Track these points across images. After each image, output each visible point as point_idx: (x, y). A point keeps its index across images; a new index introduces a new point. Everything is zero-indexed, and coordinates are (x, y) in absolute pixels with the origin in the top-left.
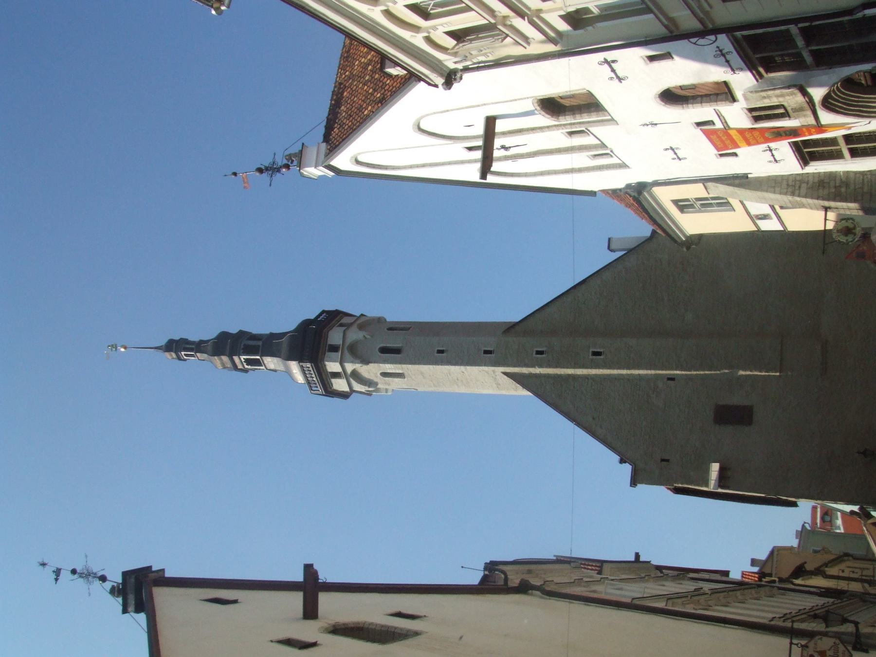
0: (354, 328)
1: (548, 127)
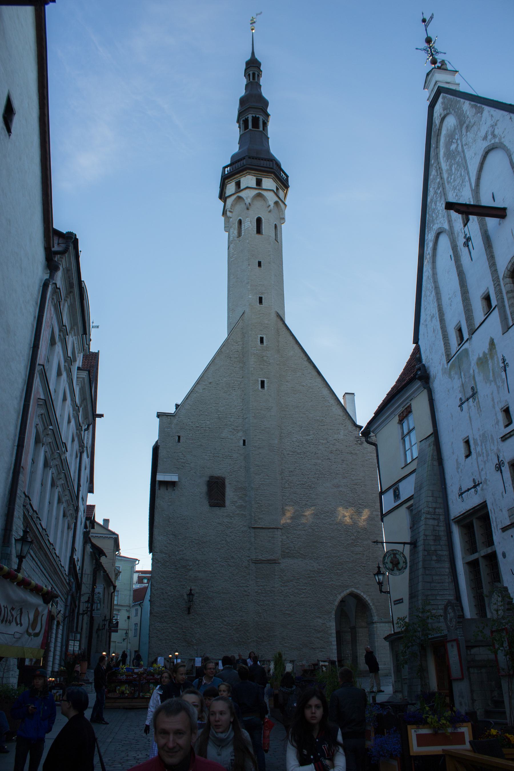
0: (276, 199)
1: (496, 271)
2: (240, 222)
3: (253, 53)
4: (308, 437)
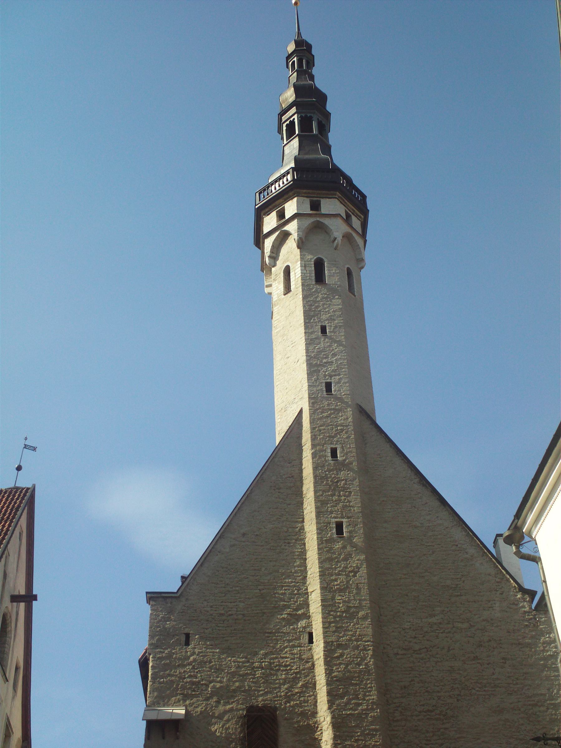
0: (345, 228)
3: (299, 34)
4: (434, 620)
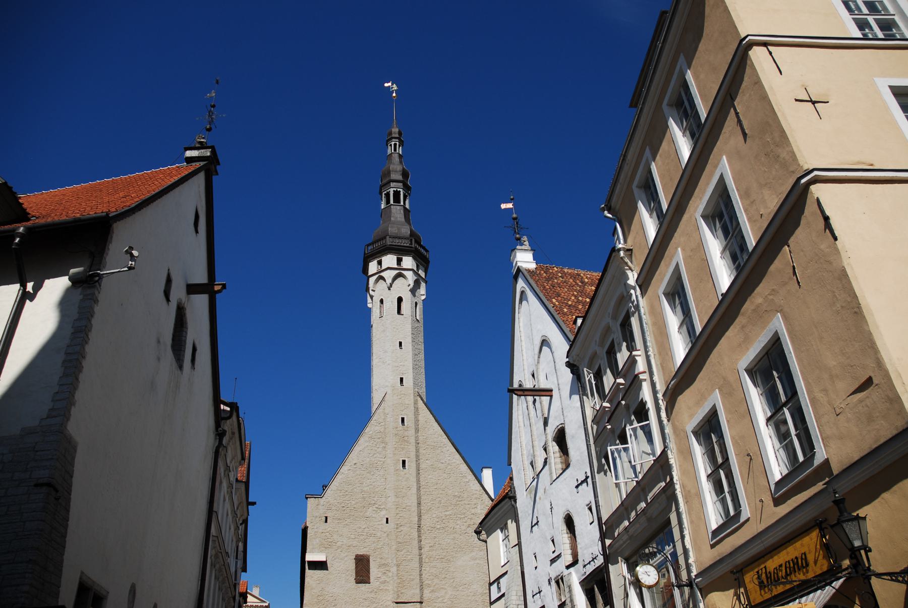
2: (382, 301)
4: (447, 513)
